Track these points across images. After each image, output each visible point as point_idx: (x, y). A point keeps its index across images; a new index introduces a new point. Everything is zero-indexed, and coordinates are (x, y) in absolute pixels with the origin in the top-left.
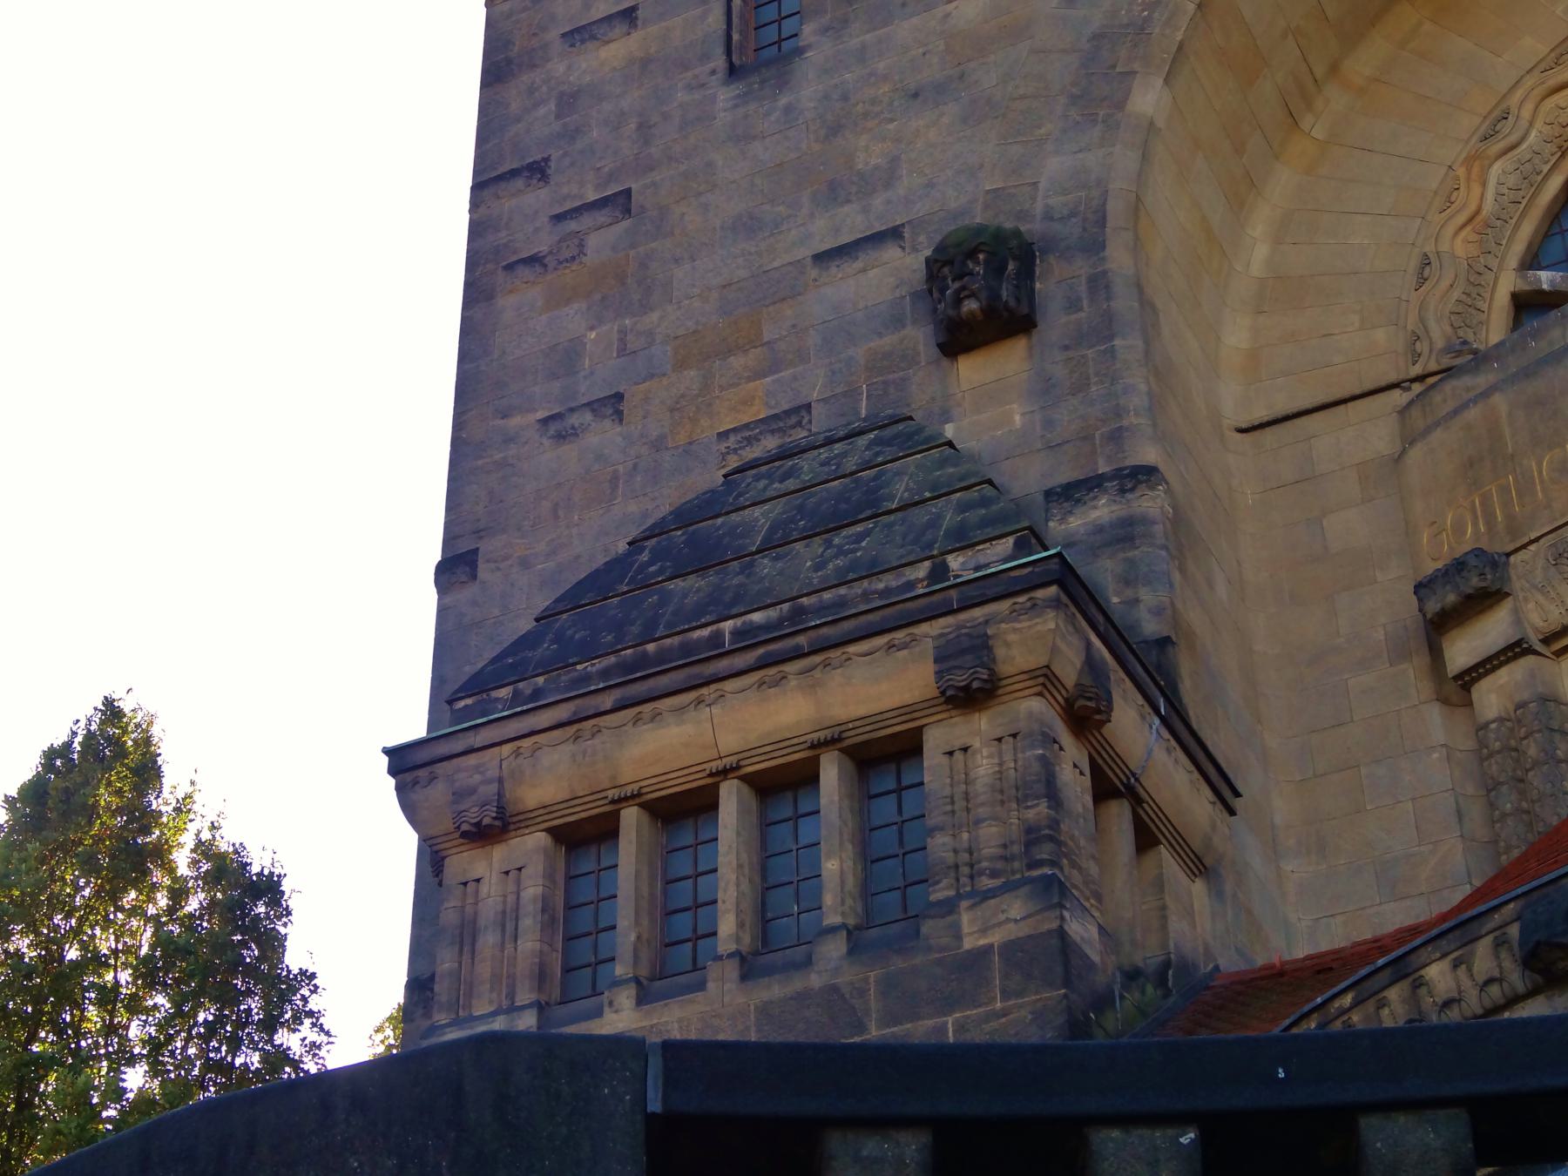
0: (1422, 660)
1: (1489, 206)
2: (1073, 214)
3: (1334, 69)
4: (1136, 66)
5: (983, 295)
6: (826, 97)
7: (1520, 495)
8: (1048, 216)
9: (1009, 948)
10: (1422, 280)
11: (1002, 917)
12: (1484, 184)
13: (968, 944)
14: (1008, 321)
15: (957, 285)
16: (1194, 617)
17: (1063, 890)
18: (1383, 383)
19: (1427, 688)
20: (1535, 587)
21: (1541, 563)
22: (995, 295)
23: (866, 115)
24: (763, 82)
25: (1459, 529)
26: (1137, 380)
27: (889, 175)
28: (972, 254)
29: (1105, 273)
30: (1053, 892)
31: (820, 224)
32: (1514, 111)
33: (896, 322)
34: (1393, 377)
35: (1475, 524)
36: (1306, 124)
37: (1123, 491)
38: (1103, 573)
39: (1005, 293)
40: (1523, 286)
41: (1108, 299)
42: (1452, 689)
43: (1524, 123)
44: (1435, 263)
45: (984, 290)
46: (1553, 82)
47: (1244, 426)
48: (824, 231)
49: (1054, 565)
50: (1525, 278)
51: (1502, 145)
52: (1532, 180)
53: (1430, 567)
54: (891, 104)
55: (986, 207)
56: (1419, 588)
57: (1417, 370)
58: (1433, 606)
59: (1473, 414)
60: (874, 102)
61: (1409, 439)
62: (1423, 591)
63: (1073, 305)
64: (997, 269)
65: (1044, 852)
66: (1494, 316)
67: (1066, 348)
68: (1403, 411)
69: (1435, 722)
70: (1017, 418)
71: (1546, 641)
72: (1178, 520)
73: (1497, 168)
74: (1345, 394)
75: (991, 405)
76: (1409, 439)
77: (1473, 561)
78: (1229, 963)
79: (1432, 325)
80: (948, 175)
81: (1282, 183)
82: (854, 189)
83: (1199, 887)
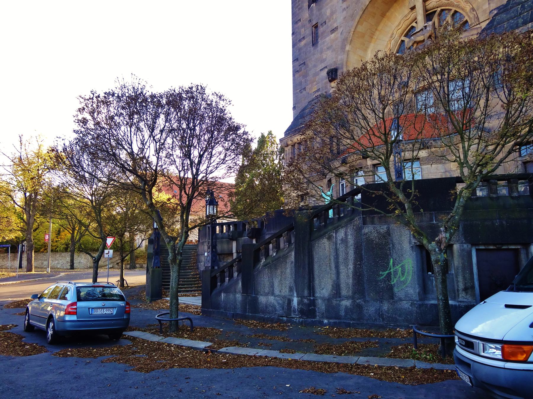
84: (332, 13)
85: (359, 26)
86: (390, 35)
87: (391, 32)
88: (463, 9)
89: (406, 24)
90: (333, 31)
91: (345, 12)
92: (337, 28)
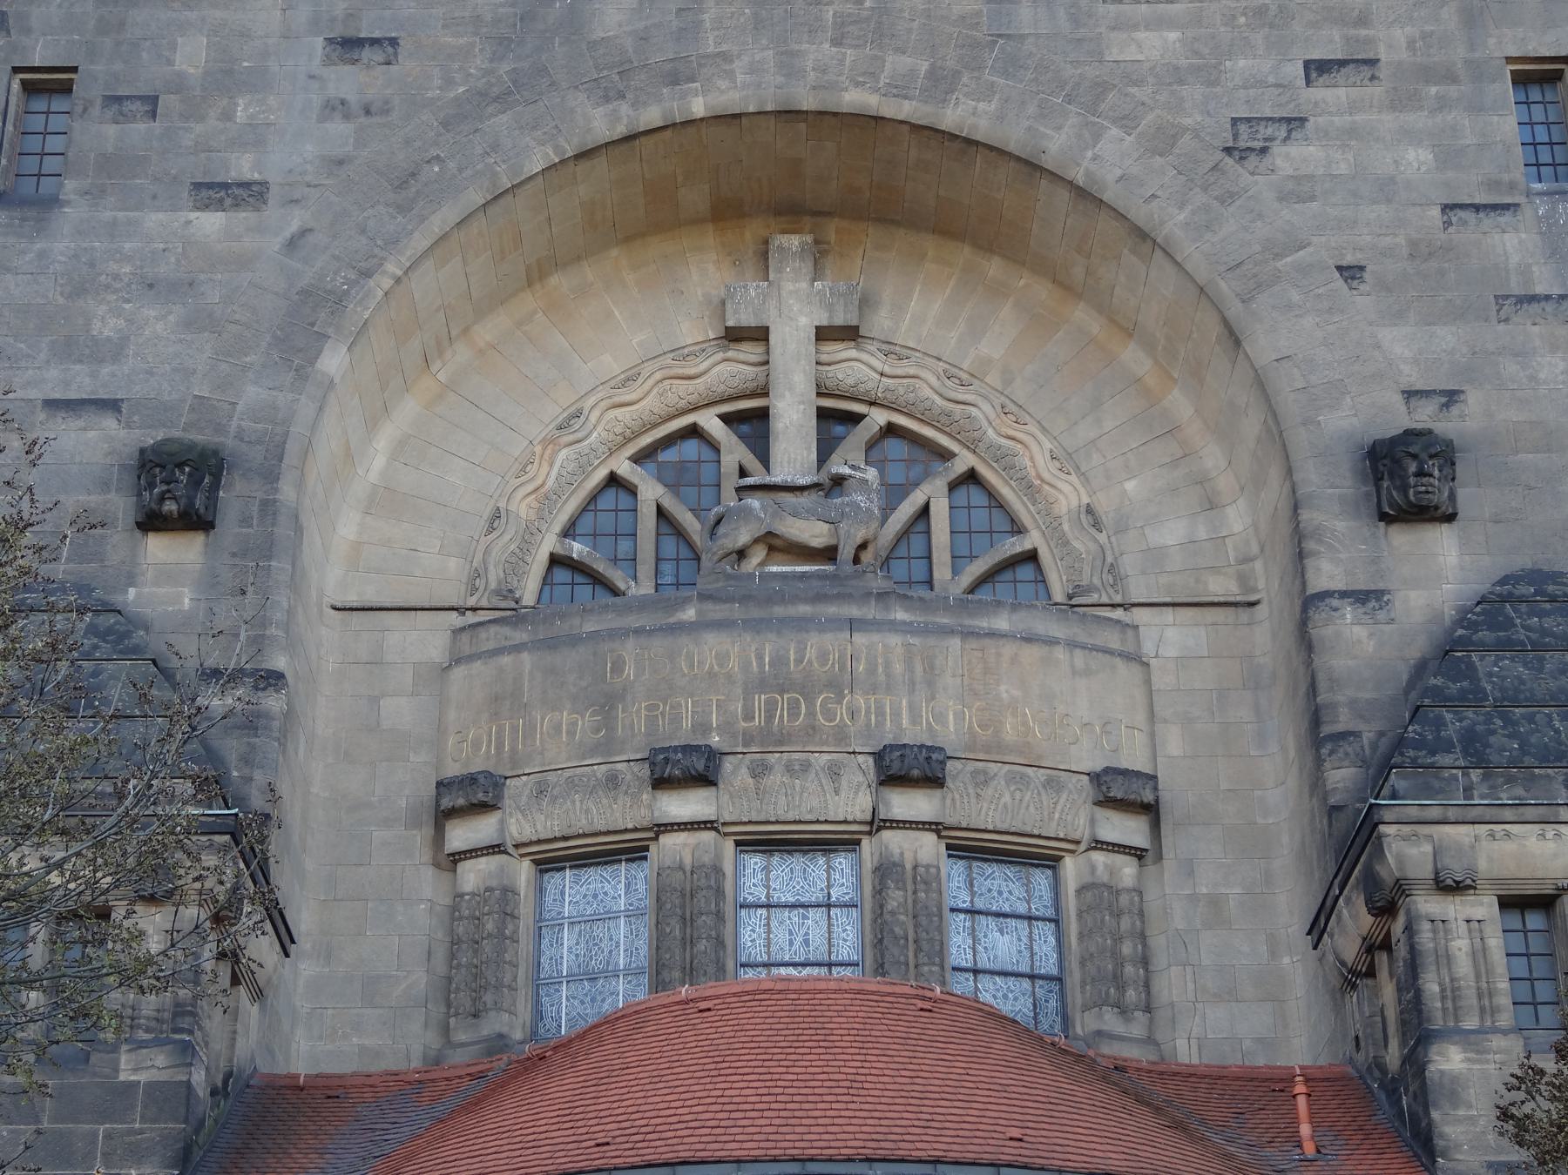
0: (428, 831)
1: (550, 483)
2: (259, 442)
3: (466, 331)
4: (330, 331)
5: (183, 501)
6: (76, 256)
7: (524, 737)
8: (239, 437)
9: (150, 1085)
10: (491, 529)
11: (150, 1063)
12: (551, 466)
13: (122, 1077)
14: (196, 521)
15: (165, 488)
16: (283, 789)
17: (194, 1053)
18: (447, 605)
19: (427, 856)
20: (518, 808)
21: (527, 792)
22: (191, 504)
23: (107, 287)
24: (23, 219)
25: (476, 745)
26: (282, 599)
27: (116, 350)
28: (180, 465)
29: (275, 501)
30: (186, 1053)
31: (53, 373)
32: (585, 412)
33: (105, 486)
34: (454, 603)
35: (489, 746)
36: (434, 369)
37: (256, 688)
38: (231, 747)
39: (199, 502)
40: (560, 551)
41: (273, 525)
42: (445, 862)
43: (590, 426)
44: (504, 520)
45: (180, 487)
46: (617, 400)
47: (339, 605)
48: (57, 380)
49: (231, 821)
50: (562, 543)
51: (571, 438)
52: (584, 469)
53: (453, 770)
54: (129, 285)
55: (192, 409)
56: (439, 784)
57: (471, 602)
58: (446, 803)
59: (506, 660)
60: (116, 277)
61: (457, 660)
62: (442, 788)
63: (245, 521)
64: (196, 482)
65: (185, 1023)
66: (534, 566)
67: (234, 555)
68: (457, 632)
69: (428, 884)
70: (187, 601)
71: (516, 846)
72: (289, 714)
73: (563, 454)
74: (419, 605)
75: (166, 578)
77: (482, 780)
78: (264, 1069)
79: (491, 568)
80: (167, 369)
81: (408, 409)
82: (87, 351)
83: (255, 1009)
84: (226, 78)
85: (429, 264)
86: (553, 412)
88: (1030, 490)
89: (672, 399)
90: (217, 193)
91: (339, 128)
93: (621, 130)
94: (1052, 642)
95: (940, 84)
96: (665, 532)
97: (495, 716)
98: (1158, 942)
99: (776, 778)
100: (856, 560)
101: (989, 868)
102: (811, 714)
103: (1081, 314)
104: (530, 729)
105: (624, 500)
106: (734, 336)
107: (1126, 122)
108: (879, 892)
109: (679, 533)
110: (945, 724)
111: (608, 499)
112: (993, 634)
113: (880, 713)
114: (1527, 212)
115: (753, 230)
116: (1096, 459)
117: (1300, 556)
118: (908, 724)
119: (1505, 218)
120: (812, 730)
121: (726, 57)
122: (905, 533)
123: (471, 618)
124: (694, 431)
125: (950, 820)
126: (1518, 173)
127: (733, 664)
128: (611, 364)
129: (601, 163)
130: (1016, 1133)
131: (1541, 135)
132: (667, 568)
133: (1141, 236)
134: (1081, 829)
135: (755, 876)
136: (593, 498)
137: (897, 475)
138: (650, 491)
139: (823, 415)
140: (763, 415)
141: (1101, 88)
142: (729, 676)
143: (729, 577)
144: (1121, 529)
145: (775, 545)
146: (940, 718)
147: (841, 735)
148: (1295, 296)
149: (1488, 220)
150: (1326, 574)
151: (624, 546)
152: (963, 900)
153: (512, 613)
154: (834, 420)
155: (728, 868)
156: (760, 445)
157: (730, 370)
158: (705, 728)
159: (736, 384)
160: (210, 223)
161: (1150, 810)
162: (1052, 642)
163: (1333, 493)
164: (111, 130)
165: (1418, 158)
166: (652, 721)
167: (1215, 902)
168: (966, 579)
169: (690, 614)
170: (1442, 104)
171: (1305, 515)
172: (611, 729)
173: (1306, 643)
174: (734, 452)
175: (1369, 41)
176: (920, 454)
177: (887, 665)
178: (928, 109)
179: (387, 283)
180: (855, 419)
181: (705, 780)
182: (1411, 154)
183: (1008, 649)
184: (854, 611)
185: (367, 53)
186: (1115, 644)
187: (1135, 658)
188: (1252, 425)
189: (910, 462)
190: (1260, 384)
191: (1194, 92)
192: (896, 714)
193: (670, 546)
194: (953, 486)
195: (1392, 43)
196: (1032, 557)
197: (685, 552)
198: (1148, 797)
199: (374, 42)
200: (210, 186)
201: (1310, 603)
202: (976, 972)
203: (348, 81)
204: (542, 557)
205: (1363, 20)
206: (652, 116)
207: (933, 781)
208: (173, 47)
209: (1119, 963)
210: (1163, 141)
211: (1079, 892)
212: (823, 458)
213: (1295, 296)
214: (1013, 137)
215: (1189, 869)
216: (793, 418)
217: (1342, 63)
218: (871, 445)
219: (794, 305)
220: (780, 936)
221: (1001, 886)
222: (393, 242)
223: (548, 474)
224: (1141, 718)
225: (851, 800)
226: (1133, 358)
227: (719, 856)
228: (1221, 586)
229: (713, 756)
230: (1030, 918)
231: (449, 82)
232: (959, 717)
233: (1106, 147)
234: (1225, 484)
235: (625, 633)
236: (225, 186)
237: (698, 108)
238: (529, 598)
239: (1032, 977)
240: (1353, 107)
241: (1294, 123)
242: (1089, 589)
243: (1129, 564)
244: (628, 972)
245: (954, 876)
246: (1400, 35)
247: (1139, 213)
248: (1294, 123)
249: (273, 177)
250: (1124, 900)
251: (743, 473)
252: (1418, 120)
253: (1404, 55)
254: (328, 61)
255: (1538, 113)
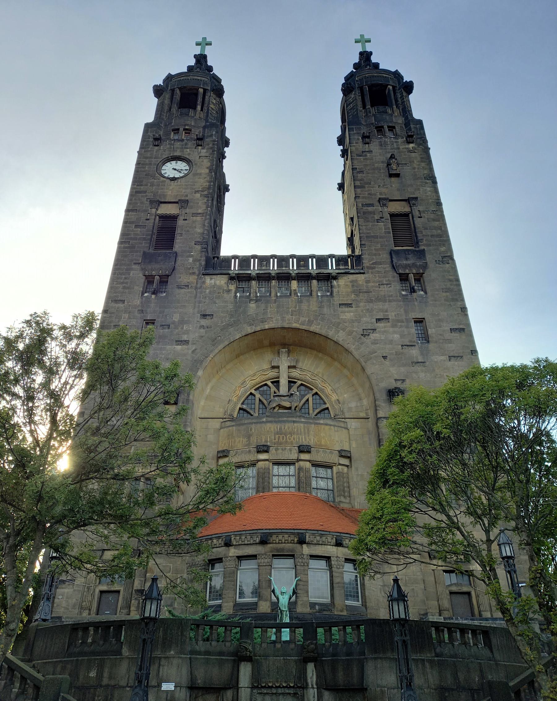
52: (246, 392)
53: (220, 449)
58: (219, 456)
59: (231, 428)
61: (221, 428)
76: (221, 428)
81: (214, 380)
84: (182, 322)
85: (218, 355)
86: (240, 381)
87: (242, 378)
88: (327, 396)
89: (262, 379)
90: (180, 342)
91: (202, 330)
92: (186, 342)
93: (253, 331)
94: (331, 425)
95: (310, 323)
96: (261, 404)
97: (228, 439)
98: (351, 483)
99: (280, 451)
100: (295, 409)
101: (320, 469)
102: (286, 439)
103: (336, 364)
104: (235, 442)
105: (253, 397)
106: (273, 367)
107: (344, 330)
108: (299, 473)
109: (263, 404)
110: (311, 440)
111: (250, 397)
112: (320, 424)
113: (299, 439)
114: (417, 346)
115: (277, 348)
116: (339, 390)
117: (376, 410)
118: (304, 441)
119: (413, 348)
120: (286, 442)
121: (272, 318)
122: (304, 404)
123: (224, 420)
124: (266, 385)
125: (312, 459)
126: (415, 339)
127: (272, 429)
128: (251, 372)
129: (249, 336)
130: (322, 524)
131: (420, 332)
132: (261, 410)
133: (347, 350)
134: (336, 461)
135: (276, 470)
136: (248, 397)
137: (303, 393)
138: (258, 396)
139: (289, 382)
140: (278, 382)
141: (339, 323)
142: (271, 431)
143: (271, 413)
144: (344, 403)
145: (280, 407)
146: (310, 440)
147: (292, 443)
148: (375, 362)
149: (410, 348)
150: (381, 414)
151: (253, 406)
152: (315, 475)
153: (232, 419)
154: (291, 383)
155: (271, 469)
156: (278, 388)
157: (272, 374)
158: (266, 441)
159: (274, 376)
160: (179, 347)
161: (349, 458)
162: (331, 425)
163: (382, 397)
164: (162, 331)
165: (397, 336)
166: (257, 440)
167: (362, 475)
168: (315, 413)
169: (264, 420)
170: (401, 326)
171: (377, 402)
172: (250, 442)
173: (378, 427)
174: (273, 389)
175: (388, 315)
176: (307, 389)
177: (300, 430)
178: (308, 327)
179: (210, 359)
180: (295, 382)
181: (267, 451)
182: (396, 336)
183: (323, 427)
184: (294, 419)
185: (207, 317)
186: (343, 426)
187: (347, 428)
188: (367, 385)
189: (305, 391)
190: (368, 377)
191: (356, 324)
192: (302, 439)
193: (261, 406)
194: (313, 395)
195: (392, 315)
196: (327, 408)
197: (264, 407)
198: (349, 455)
199: (209, 315)
200: (179, 341)
201: (378, 419)
202: (317, 489)
203: (204, 322)
204: (238, 408)
205: (386, 311)
206: (258, 328)
207: (309, 452)
208: (173, 316)
209: (344, 487)
210: (350, 333)
211: (336, 473)
212: (289, 390)
213: (375, 362)
214: (323, 332)
215: (357, 469)
216: (284, 382)
217: (383, 319)
218: (298, 387)
219: (284, 362)
220: (280, 482)
221: (322, 472)
222: (212, 351)
223: (239, 393)
224: (348, 440)
225: (294, 455)
226: (345, 371)
227: (269, 466)
228: (363, 415)
229: (268, 447)
230: (327, 478)
231: (222, 322)
232: (314, 440)
233: (340, 334)
234: (363, 395)
235: (252, 423)
236: (182, 341)
237: (267, 327)
238: (235, 416)
239: (328, 490)
240: (385, 327)
241: (374, 330)
242: (338, 415)
243: (345, 410)
244: (252, 488)
245: (313, 469)
246: (393, 314)
247: (346, 346)
248: (374, 330)
249: (190, 340)
250: (345, 475)
251: (275, 393)
252: (396, 329)
253: (394, 318)
254: (201, 318)
255: (419, 328)
